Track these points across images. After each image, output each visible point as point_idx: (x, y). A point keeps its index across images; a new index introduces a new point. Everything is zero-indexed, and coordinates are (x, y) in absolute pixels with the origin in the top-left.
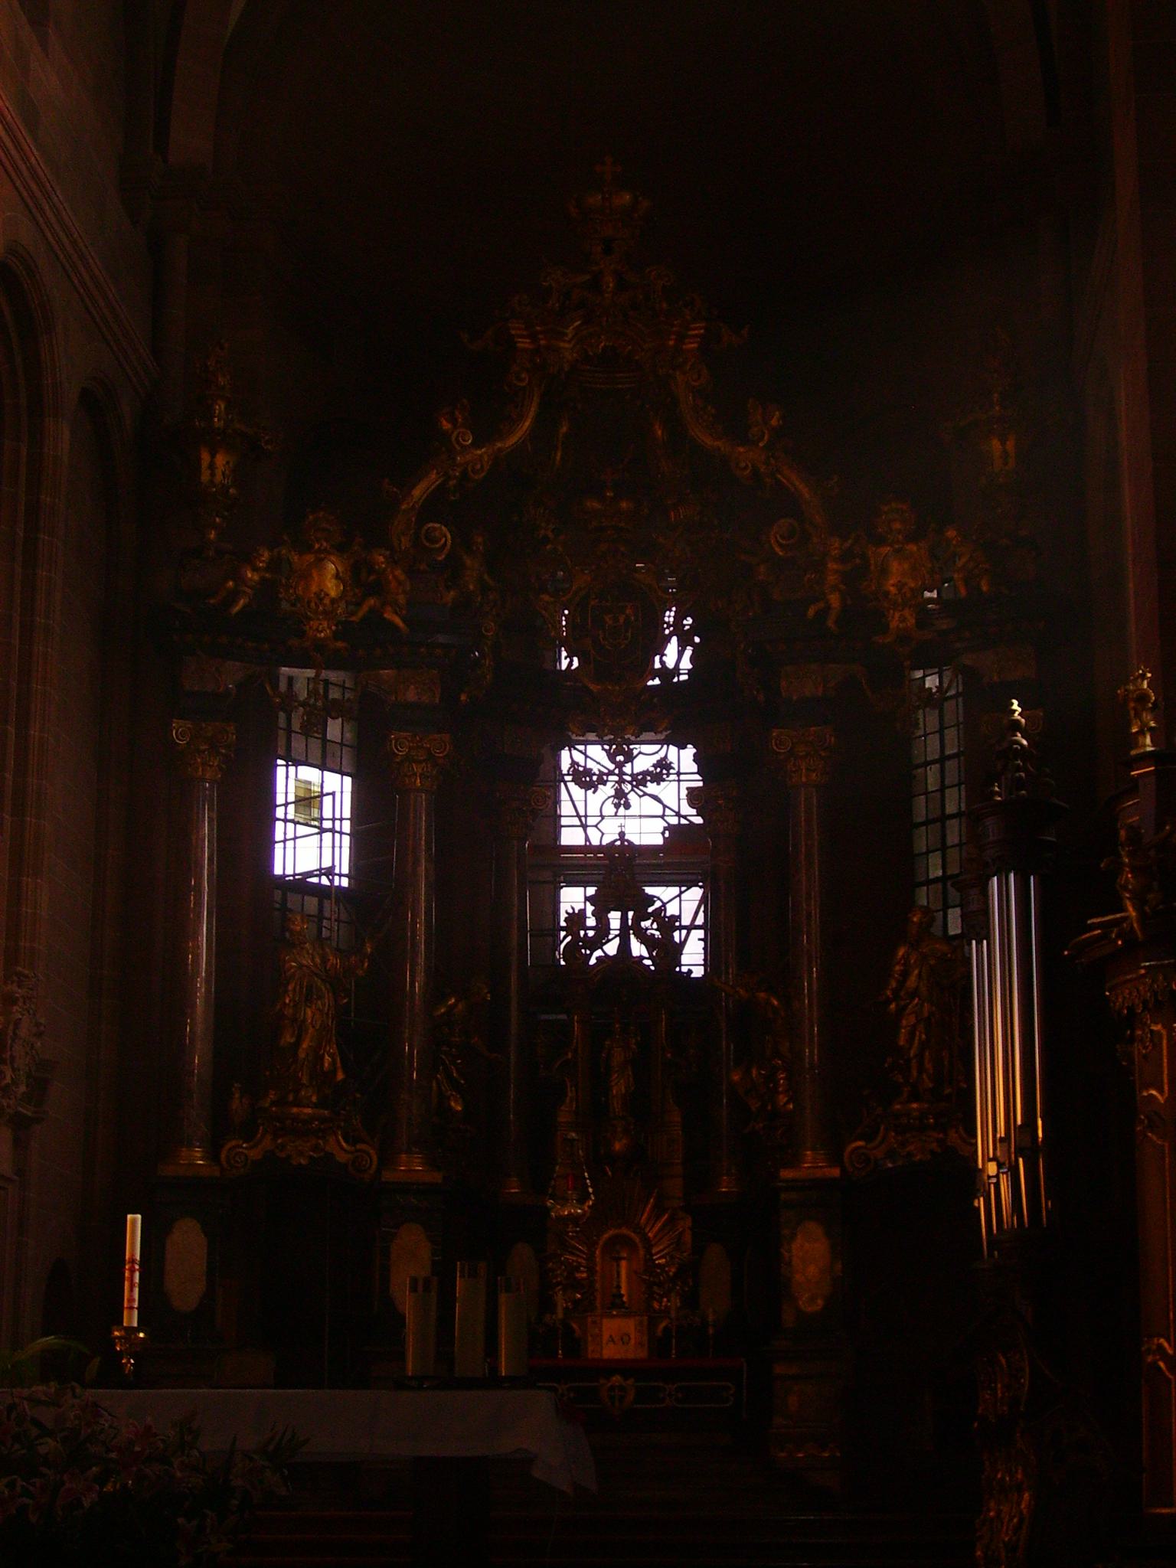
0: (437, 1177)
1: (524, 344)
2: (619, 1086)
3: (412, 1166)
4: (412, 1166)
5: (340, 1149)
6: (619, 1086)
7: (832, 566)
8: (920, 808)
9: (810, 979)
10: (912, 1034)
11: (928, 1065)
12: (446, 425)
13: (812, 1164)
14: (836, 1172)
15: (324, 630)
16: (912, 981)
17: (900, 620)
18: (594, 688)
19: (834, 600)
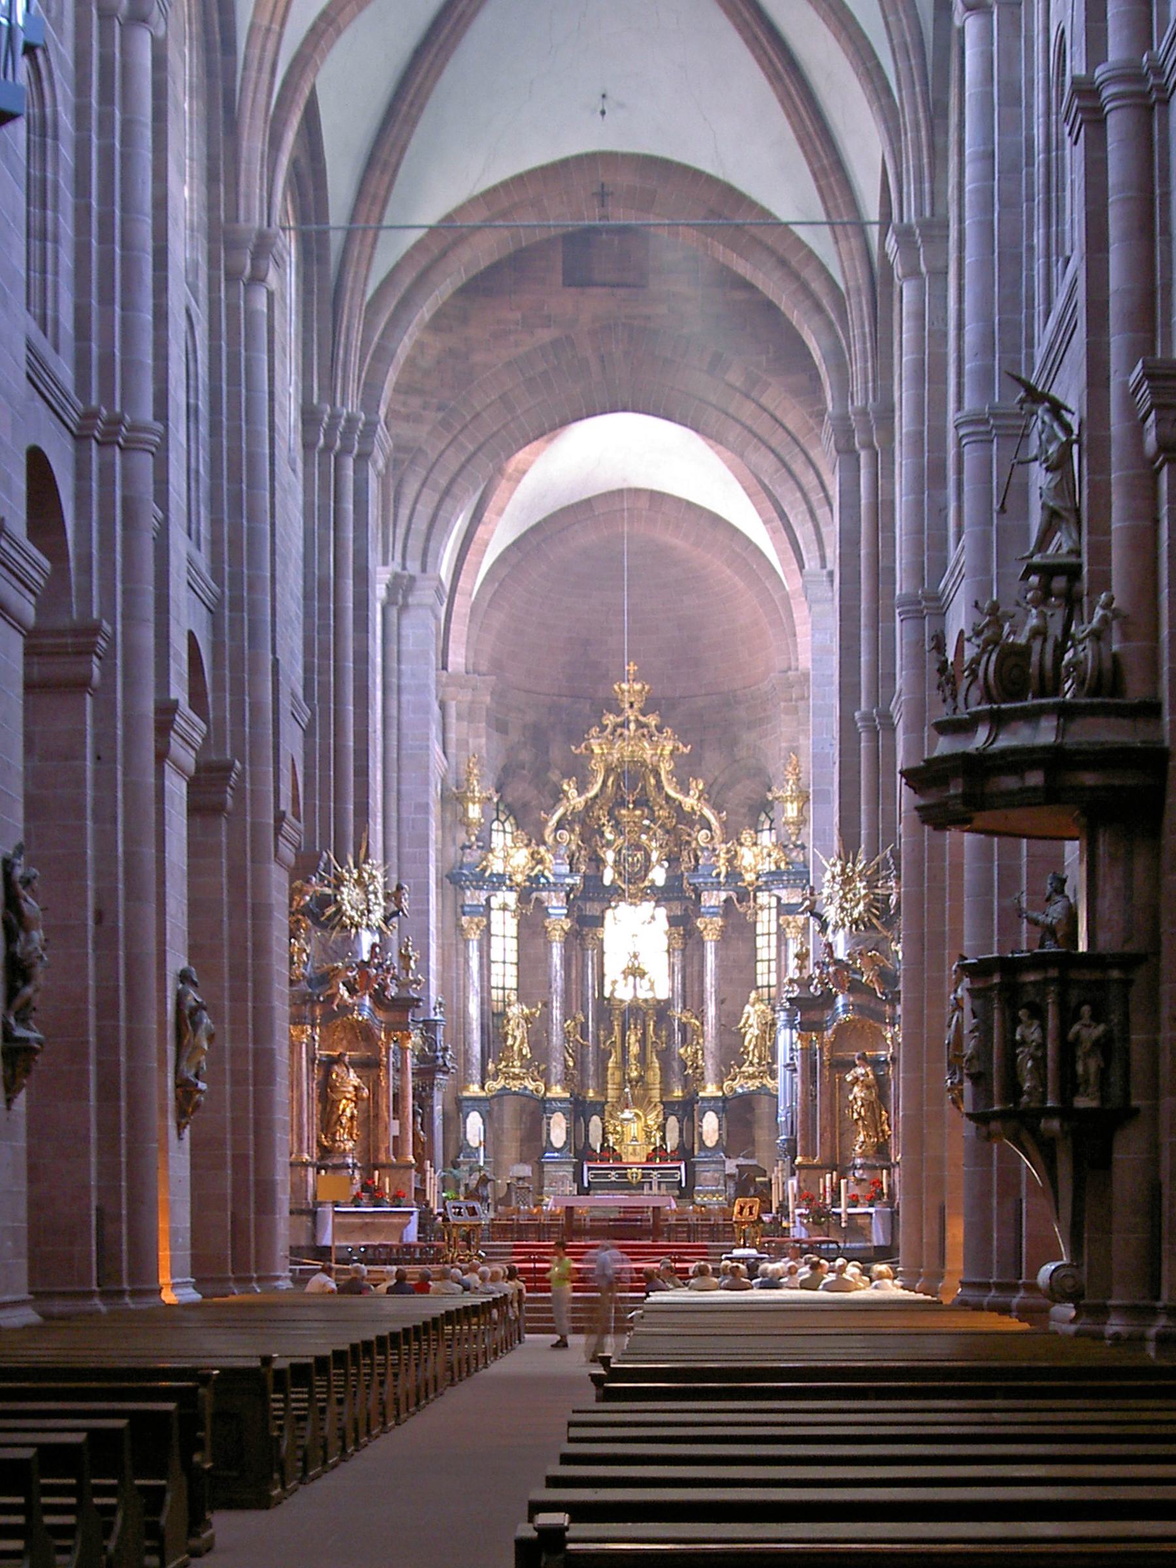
0: (568, 1095)
1: (597, 750)
2: (634, 1049)
3: (557, 1091)
4: (557, 1091)
5: (531, 1085)
6: (634, 1049)
7: (722, 855)
8: (760, 929)
9: (711, 1010)
10: (750, 1041)
11: (756, 1053)
12: (566, 787)
13: (711, 1090)
14: (720, 1094)
15: (519, 878)
16: (750, 1022)
17: (749, 877)
18: (623, 886)
19: (723, 870)
